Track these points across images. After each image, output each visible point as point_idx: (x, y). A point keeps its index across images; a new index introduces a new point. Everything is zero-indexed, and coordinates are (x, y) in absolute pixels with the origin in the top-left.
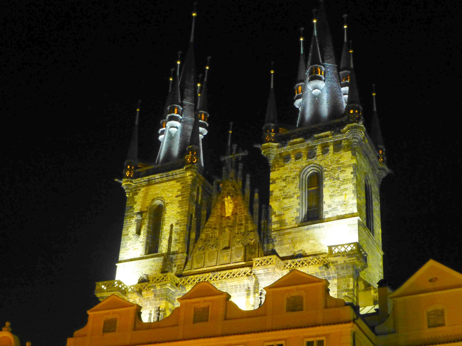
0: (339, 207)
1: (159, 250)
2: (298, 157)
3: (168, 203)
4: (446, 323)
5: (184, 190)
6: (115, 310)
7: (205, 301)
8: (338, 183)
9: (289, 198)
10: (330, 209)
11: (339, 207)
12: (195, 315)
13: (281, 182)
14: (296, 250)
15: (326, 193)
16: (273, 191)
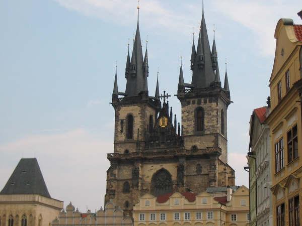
2: (194, 103)
8: (210, 116)
15: (206, 121)
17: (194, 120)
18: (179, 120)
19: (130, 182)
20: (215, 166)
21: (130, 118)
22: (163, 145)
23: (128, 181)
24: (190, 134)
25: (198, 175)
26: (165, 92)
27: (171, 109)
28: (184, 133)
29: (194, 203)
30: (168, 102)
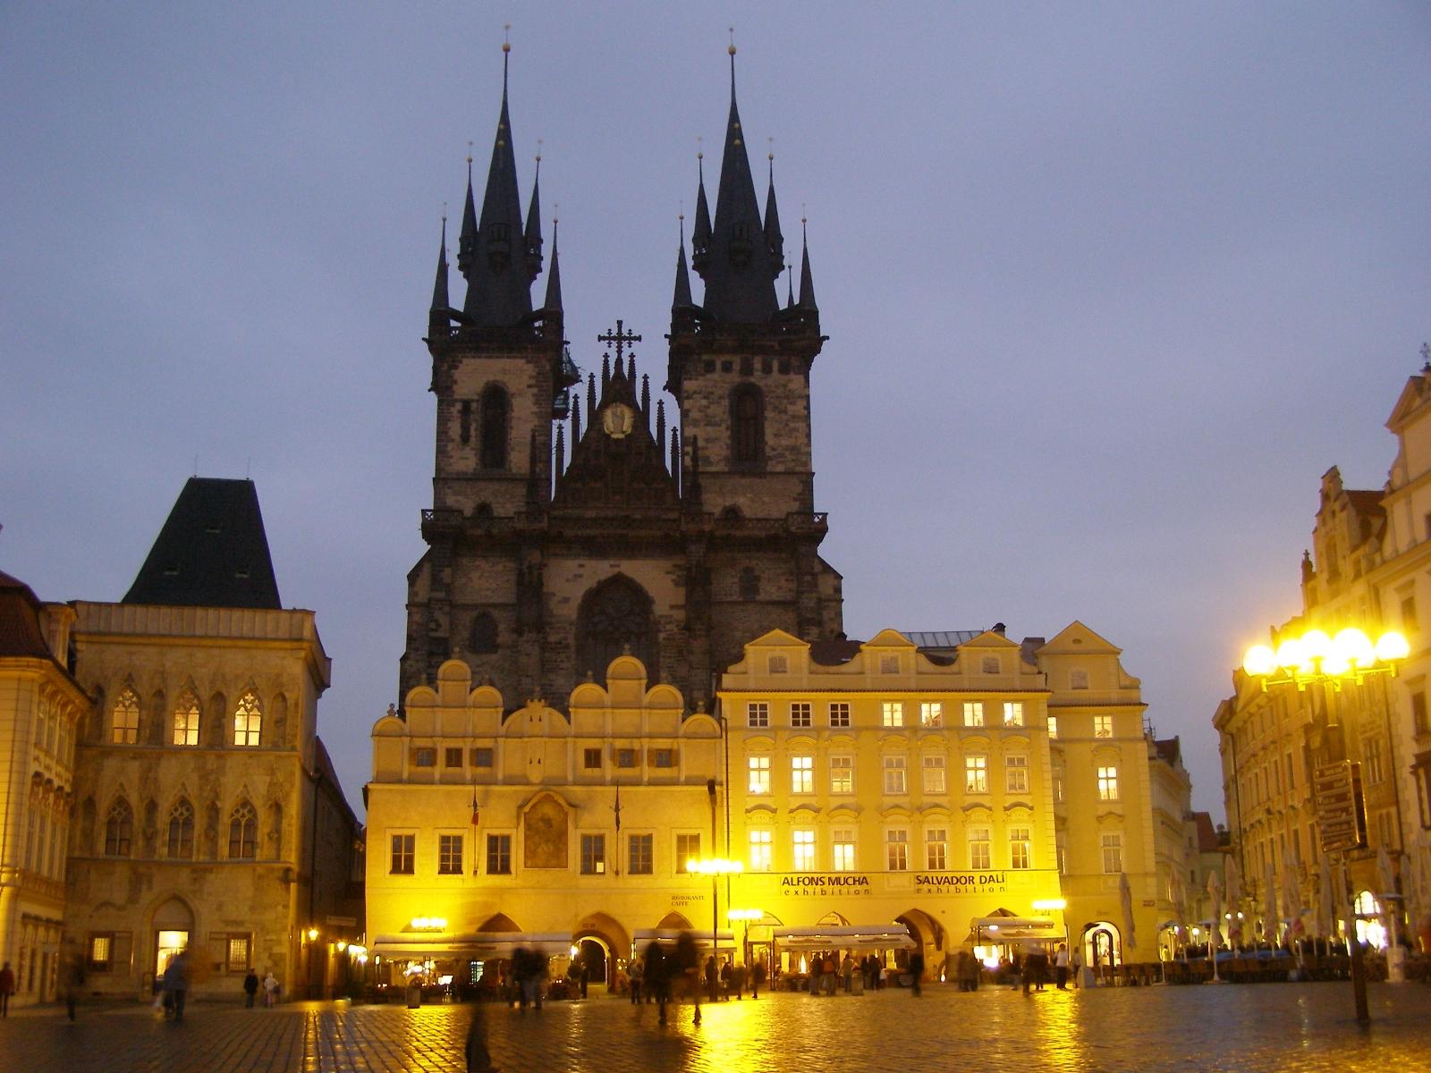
0: (787, 453)
1: (507, 466)
2: (727, 368)
3: (513, 395)
4: (1089, 686)
5: (541, 379)
6: (785, 647)
7: (893, 651)
8: (784, 417)
9: (715, 424)
10: (774, 453)
11: (787, 453)
12: (883, 665)
13: (701, 399)
14: (727, 504)
16: (688, 411)
17: (729, 423)
18: (673, 418)
19: (496, 614)
20: (814, 575)
21: (496, 398)
22: (618, 497)
23: (491, 610)
24: (713, 469)
25: (745, 603)
26: (620, 323)
27: (646, 384)
28: (700, 463)
29: (954, 668)
30: (632, 356)
